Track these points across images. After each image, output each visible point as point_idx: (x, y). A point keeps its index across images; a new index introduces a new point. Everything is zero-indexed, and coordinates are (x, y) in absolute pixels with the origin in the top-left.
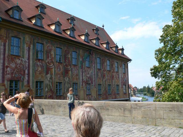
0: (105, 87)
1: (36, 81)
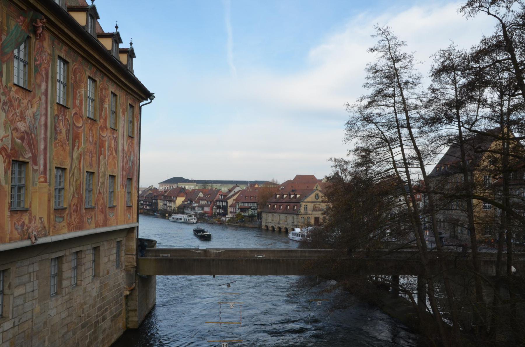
0: (77, 180)
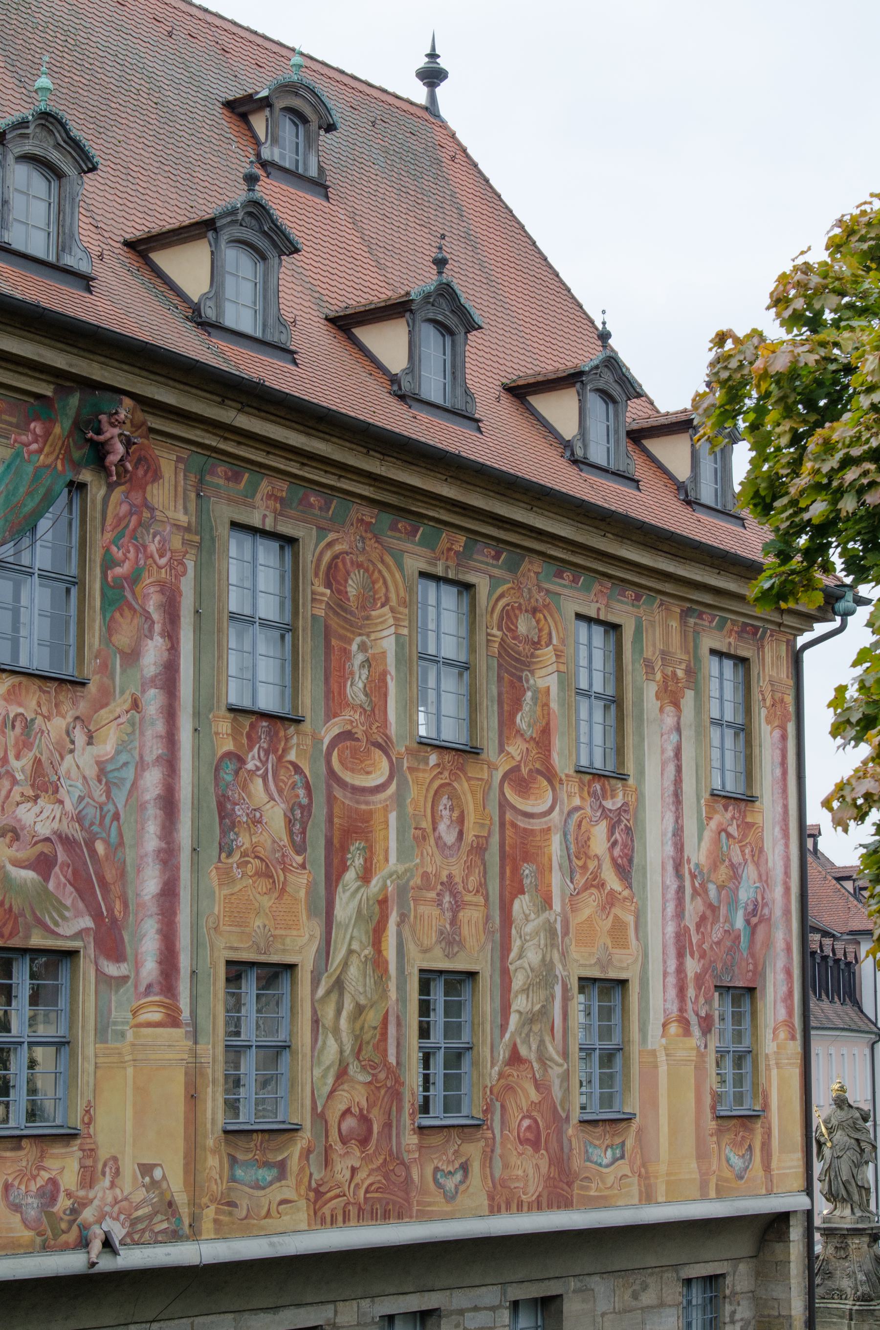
0: (359, 1010)
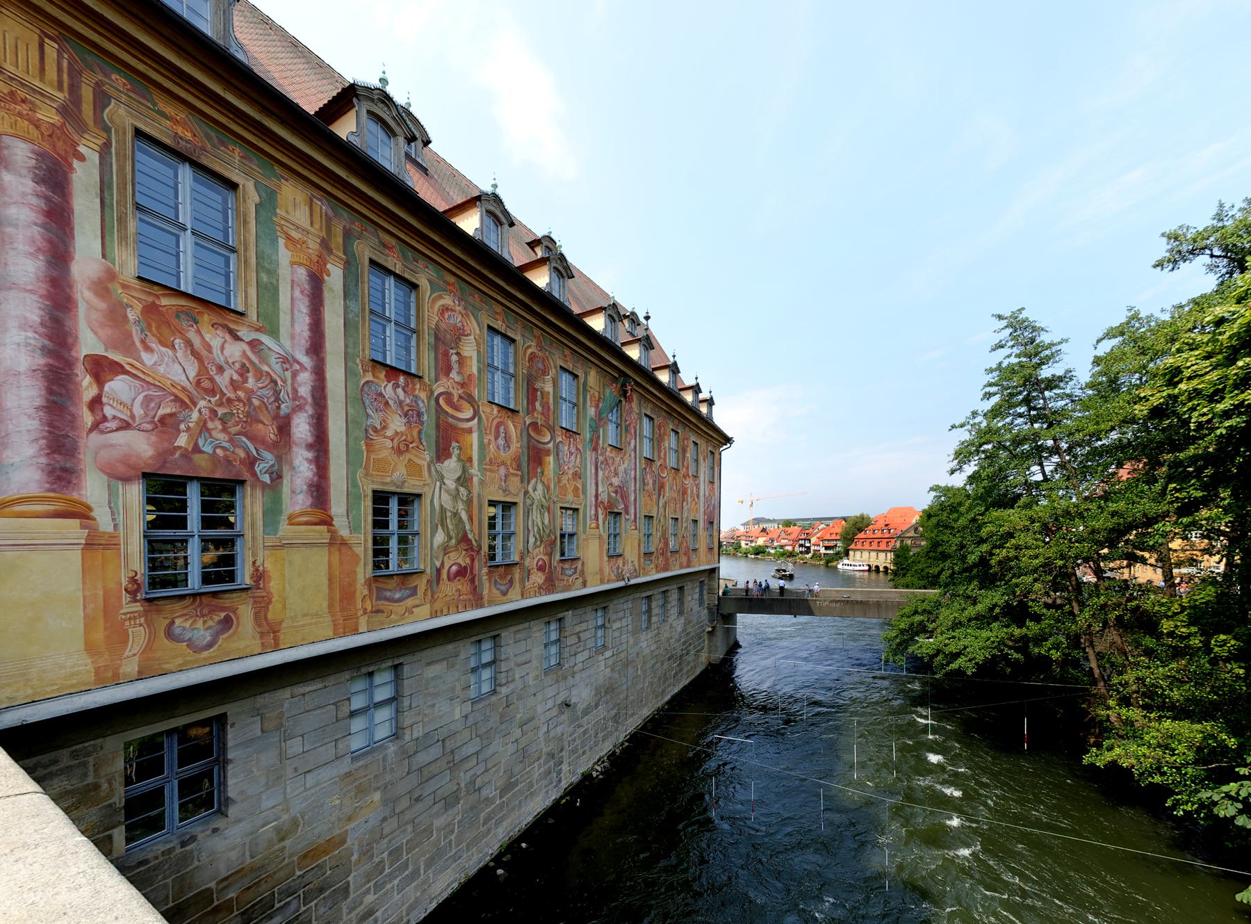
1: (374, 492)
